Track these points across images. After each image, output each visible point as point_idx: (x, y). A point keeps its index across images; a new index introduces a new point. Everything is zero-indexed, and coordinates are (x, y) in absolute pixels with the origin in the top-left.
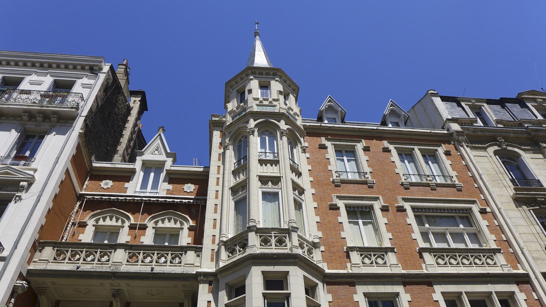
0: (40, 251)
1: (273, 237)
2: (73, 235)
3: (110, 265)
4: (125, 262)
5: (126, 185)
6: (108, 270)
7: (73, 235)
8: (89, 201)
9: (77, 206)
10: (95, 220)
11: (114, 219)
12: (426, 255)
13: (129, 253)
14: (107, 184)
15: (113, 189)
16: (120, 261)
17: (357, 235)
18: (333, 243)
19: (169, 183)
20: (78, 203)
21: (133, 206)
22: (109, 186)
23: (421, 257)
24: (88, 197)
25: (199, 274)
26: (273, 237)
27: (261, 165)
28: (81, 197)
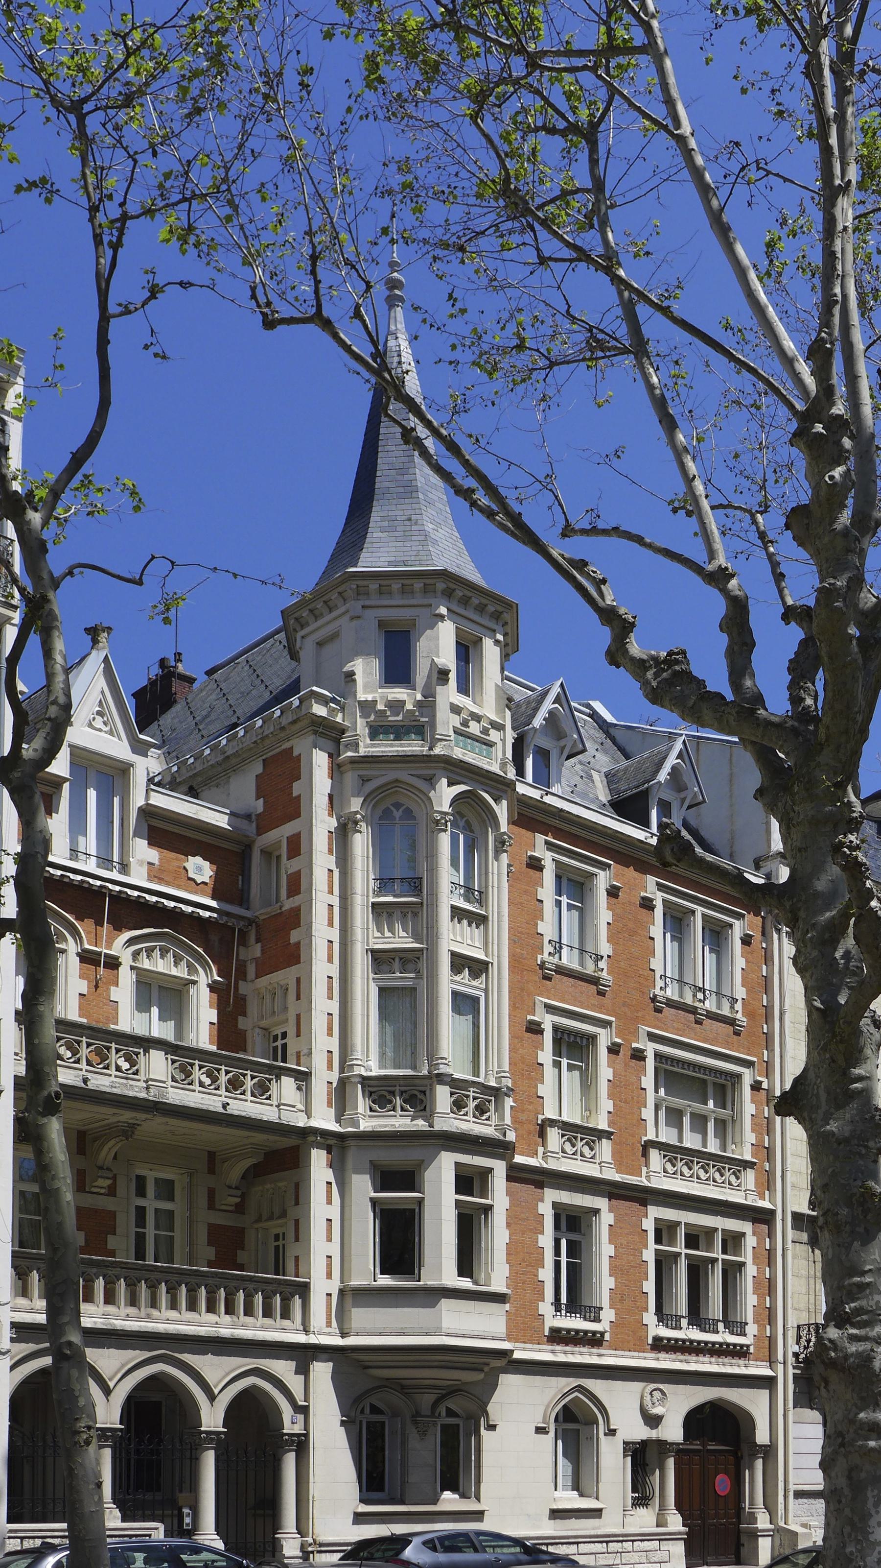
12: (655, 1155)
23: (645, 1154)
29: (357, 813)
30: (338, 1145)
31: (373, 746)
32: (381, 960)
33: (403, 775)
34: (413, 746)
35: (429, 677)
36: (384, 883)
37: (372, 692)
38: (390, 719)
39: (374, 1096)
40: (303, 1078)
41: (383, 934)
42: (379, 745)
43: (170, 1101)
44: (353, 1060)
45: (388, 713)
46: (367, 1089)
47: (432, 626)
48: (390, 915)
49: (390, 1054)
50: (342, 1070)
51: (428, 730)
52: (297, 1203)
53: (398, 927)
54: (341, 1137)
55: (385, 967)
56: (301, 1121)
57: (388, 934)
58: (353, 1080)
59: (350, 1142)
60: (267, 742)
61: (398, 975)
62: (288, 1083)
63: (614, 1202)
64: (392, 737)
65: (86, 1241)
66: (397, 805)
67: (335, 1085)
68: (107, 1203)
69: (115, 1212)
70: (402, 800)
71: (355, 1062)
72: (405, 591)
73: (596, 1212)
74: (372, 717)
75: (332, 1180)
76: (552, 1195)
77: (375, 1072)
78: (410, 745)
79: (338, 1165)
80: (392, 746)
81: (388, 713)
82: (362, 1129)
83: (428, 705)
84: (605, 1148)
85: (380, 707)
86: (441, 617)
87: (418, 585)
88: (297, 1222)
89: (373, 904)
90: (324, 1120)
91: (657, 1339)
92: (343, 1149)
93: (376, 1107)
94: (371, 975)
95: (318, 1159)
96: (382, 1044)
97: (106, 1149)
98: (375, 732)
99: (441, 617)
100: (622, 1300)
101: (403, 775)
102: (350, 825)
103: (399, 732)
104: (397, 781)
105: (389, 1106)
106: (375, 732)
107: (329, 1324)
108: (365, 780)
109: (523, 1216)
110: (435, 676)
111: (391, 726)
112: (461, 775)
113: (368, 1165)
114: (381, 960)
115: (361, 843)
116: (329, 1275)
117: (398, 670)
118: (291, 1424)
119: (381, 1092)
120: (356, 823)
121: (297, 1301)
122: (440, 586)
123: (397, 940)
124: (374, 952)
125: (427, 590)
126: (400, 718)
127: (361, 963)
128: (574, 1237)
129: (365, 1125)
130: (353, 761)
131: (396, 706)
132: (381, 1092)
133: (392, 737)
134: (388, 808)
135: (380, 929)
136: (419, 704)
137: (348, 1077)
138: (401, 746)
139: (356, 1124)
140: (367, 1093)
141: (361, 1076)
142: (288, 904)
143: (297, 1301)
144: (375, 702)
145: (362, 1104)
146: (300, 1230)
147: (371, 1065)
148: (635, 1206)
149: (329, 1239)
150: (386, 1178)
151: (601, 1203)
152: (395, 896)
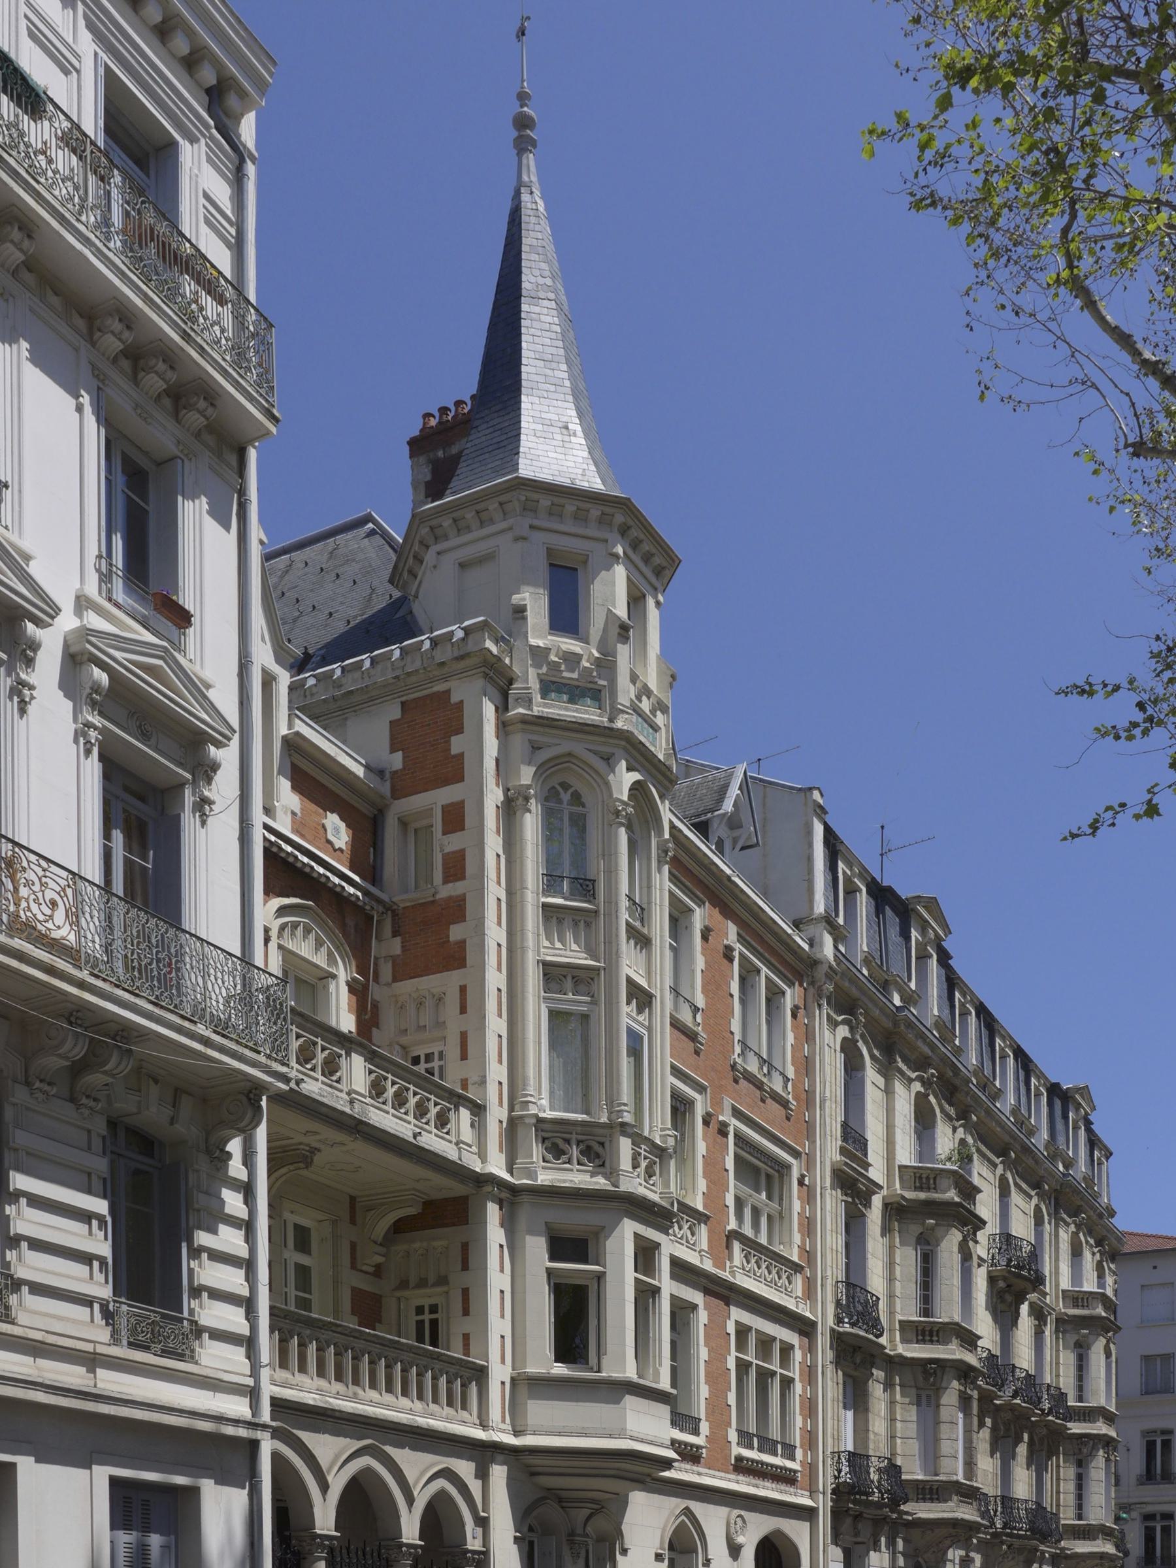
29: (529, 787)
30: (512, 1197)
31: (545, 706)
32: (553, 974)
33: (578, 748)
34: (588, 713)
35: (605, 630)
36: (552, 882)
37: (540, 637)
38: (565, 674)
39: (548, 1144)
40: (478, 1109)
41: (552, 943)
42: (552, 706)
44: (526, 1095)
45: (563, 667)
46: (540, 1133)
47: (608, 568)
48: (560, 921)
49: (560, 1093)
50: (511, 1108)
51: (606, 695)
52: (465, 1266)
53: (569, 936)
54: (514, 1190)
55: (553, 985)
56: (478, 1167)
57: (558, 945)
58: (527, 1121)
59: (525, 1198)
60: (413, 679)
61: (570, 996)
62: (465, 1114)
64: (565, 697)
66: (565, 786)
67: (505, 1125)
70: (572, 780)
71: (530, 1099)
72: (580, 517)
74: (544, 669)
75: (504, 1243)
77: (548, 1114)
78: (587, 712)
79: (509, 1224)
80: (566, 709)
81: (563, 667)
82: (539, 1182)
83: (606, 664)
85: (553, 658)
87: (595, 512)
88: (466, 1292)
89: (545, 905)
90: (496, 1166)
92: (512, 1204)
93: (550, 1157)
94: (542, 994)
95: (493, 1212)
96: (552, 1079)
98: (549, 687)
99: (617, 556)
101: (579, 749)
102: (520, 801)
103: (576, 693)
104: (570, 754)
105: (564, 1158)
106: (549, 687)
107: (503, 1421)
108: (535, 748)
110: (614, 631)
111: (565, 685)
113: (543, 1228)
114: (553, 974)
115: (531, 824)
116: (503, 1361)
117: (566, 617)
118: (474, 1543)
119: (557, 1139)
120: (527, 799)
121: (474, 1388)
122: (619, 519)
123: (568, 953)
124: (546, 965)
125: (604, 521)
126: (575, 675)
127: (532, 978)
129: (545, 1178)
130: (525, 721)
131: (572, 659)
132: (557, 1139)
133: (565, 697)
134: (553, 788)
135: (549, 938)
136: (598, 663)
137: (521, 1117)
138: (577, 711)
139: (532, 1174)
140: (540, 1140)
141: (536, 1116)
142: (446, 891)
143: (474, 1388)
144: (547, 650)
145: (537, 1151)
146: (470, 1302)
147: (543, 1104)
149: (502, 1316)
150: (567, 1246)
152: (566, 899)
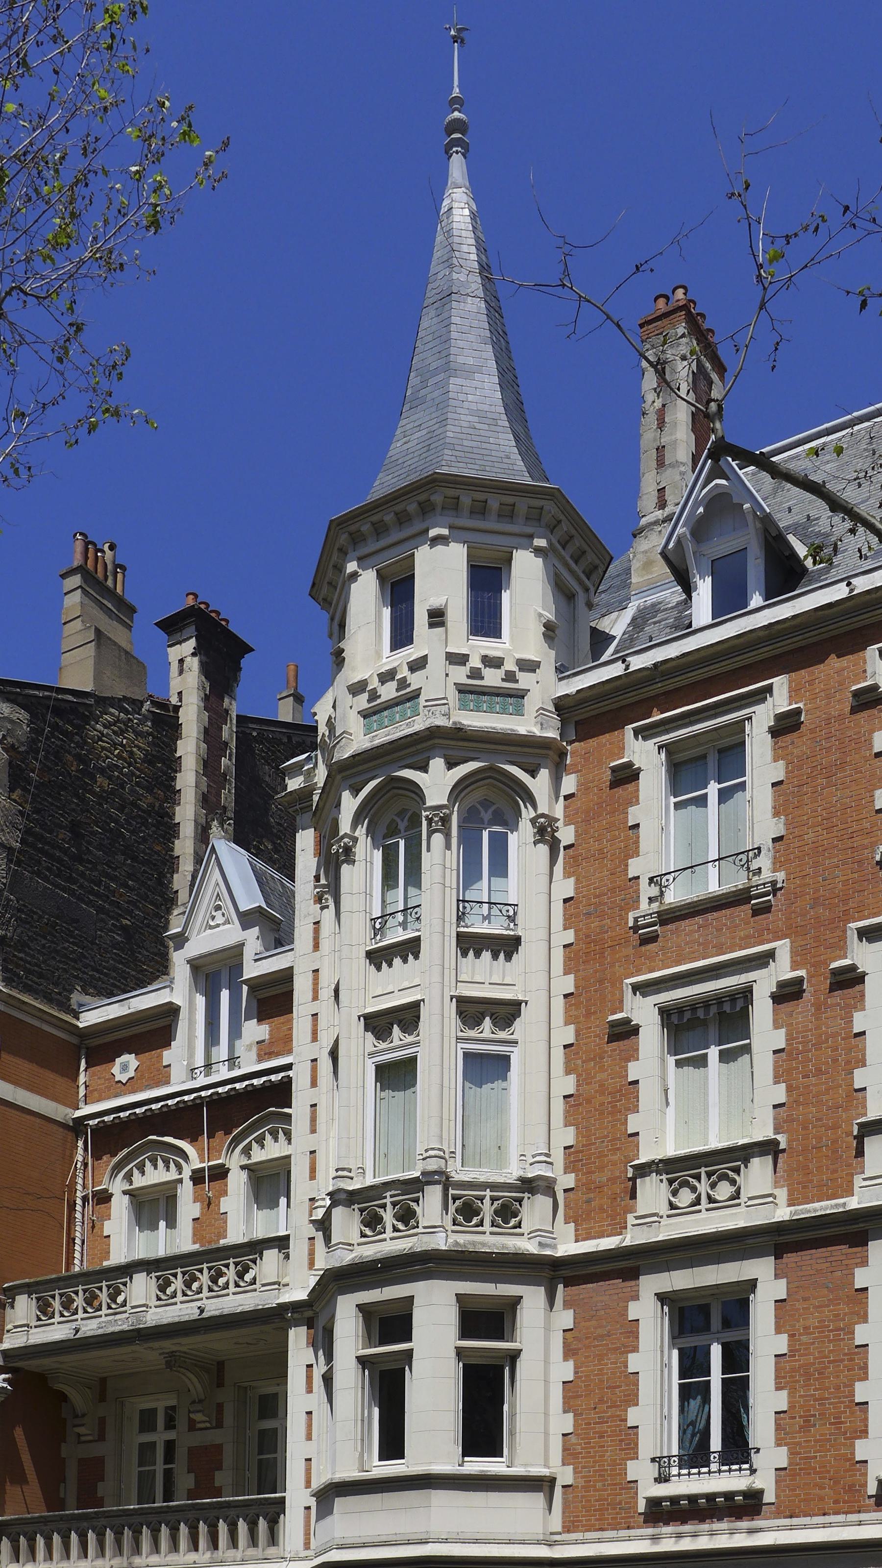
0: (13, 1307)
1: (389, 1207)
2: (93, 1227)
3: (126, 1315)
4: (154, 1302)
5: (168, 1056)
6: (125, 1327)
7: (93, 1227)
8: (95, 1130)
9: (80, 1151)
10: (124, 1177)
11: (160, 1163)
13: (158, 1278)
14: (126, 1065)
15: (142, 1077)
16: (144, 1302)
17: (684, 1106)
18: (601, 1155)
19: (260, 1020)
20: (80, 1143)
21: (187, 1118)
22: (131, 1073)
24: (91, 1122)
25: (283, 1308)
26: (389, 1207)
27: (379, 968)
28: (78, 1126)
43: (148, 1325)
63: (790, 1258)
65: (196, 1482)
68: (215, 1437)
69: (80, 1460)
73: (752, 1284)
76: (652, 1284)
84: (758, 1175)
86: (354, 576)
91: (654, 1503)
97: (195, 1380)
100: (807, 1425)
109: (599, 1331)
112: (359, 773)
128: (732, 1336)
148: (841, 1251)
151: (760, 1268)
